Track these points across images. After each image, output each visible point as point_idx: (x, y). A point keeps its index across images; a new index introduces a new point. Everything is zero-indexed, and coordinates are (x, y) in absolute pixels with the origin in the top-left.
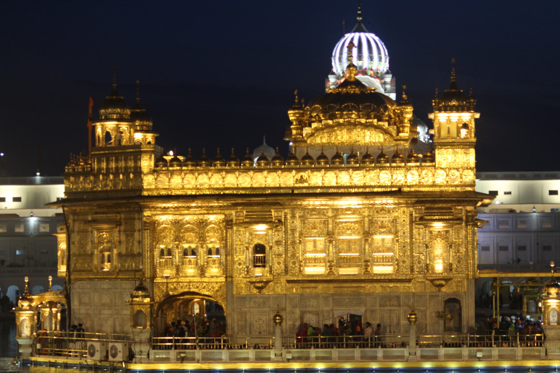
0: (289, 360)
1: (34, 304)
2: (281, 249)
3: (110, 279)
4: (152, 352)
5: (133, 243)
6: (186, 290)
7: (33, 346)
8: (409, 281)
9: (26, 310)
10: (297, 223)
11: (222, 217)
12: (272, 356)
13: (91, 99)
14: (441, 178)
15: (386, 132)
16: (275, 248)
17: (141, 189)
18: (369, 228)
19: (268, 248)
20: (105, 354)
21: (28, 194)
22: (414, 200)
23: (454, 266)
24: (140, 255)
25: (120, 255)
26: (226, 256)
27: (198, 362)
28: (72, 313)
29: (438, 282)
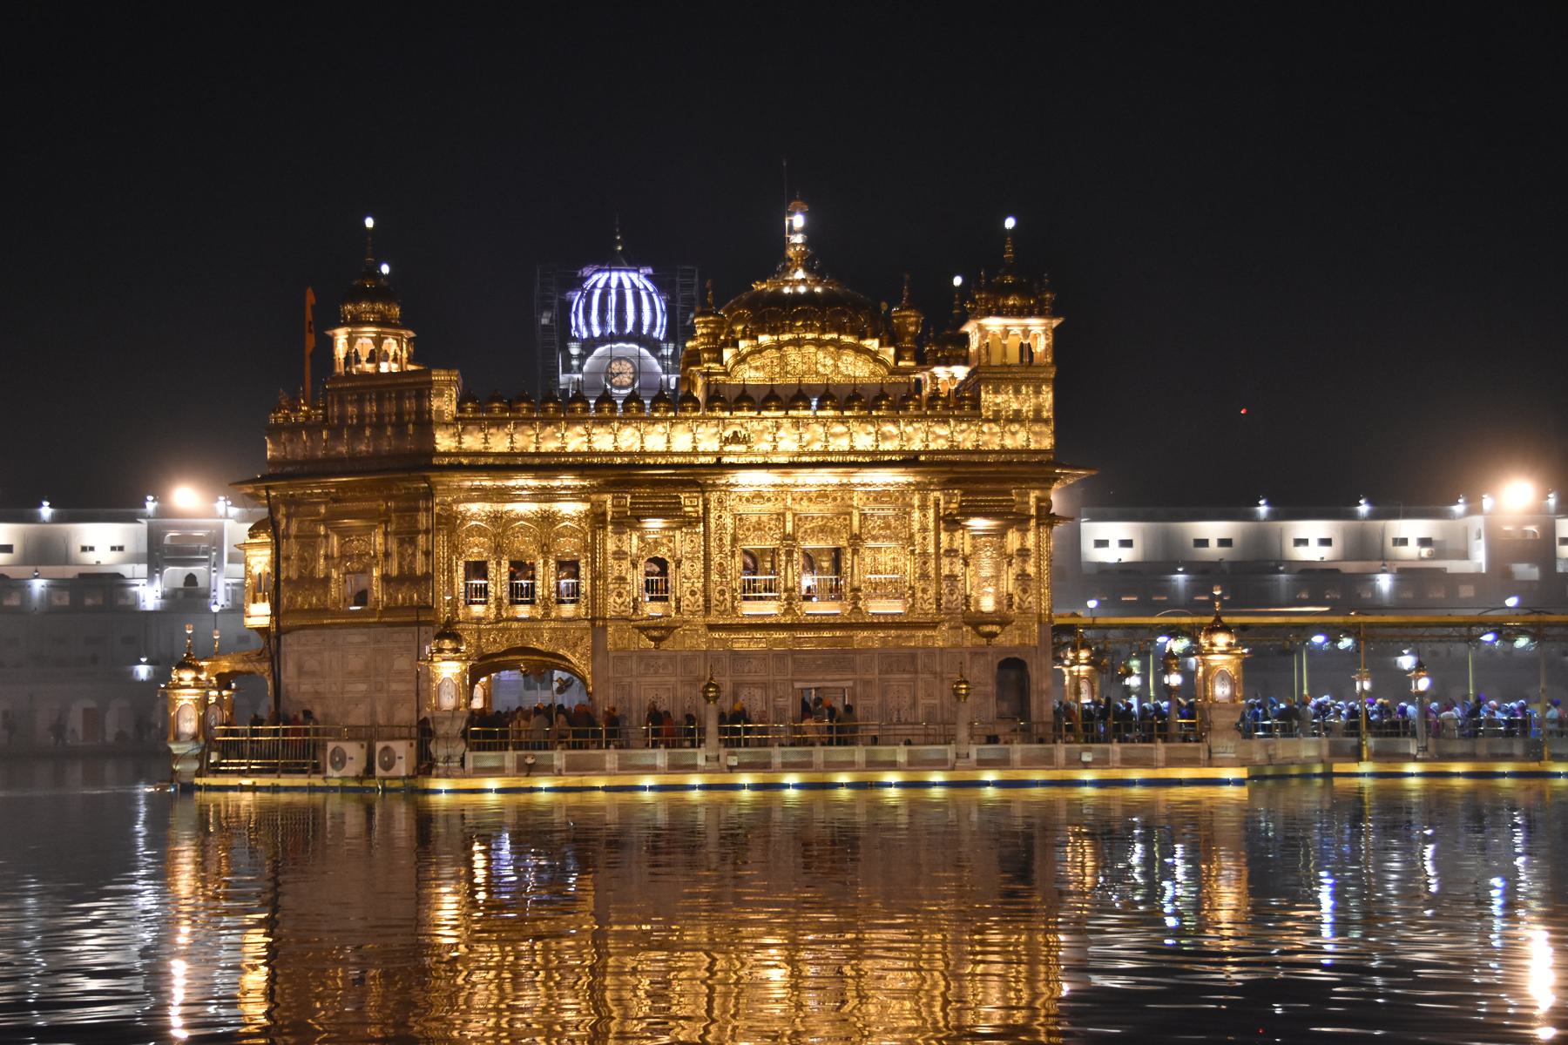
0: (731, 769)
1: (203, 676)
2: (699, 566)
3: (367, 625)
4: (470, 756)
5: (414, 555)
6: (519, 643)
7: (202, 757)
8: (934, 625)
9: (188, 687)
10: (728, 520)
11: (583, 507)
12: (701, 761)
14: (993, 438)
15: (874, 356)
19: (672, 566)
21: (26, 539)
23: (1016, 599)
24: (428, 577)
25: (386, 578)
26: (593, 580)
27: (560, 774)
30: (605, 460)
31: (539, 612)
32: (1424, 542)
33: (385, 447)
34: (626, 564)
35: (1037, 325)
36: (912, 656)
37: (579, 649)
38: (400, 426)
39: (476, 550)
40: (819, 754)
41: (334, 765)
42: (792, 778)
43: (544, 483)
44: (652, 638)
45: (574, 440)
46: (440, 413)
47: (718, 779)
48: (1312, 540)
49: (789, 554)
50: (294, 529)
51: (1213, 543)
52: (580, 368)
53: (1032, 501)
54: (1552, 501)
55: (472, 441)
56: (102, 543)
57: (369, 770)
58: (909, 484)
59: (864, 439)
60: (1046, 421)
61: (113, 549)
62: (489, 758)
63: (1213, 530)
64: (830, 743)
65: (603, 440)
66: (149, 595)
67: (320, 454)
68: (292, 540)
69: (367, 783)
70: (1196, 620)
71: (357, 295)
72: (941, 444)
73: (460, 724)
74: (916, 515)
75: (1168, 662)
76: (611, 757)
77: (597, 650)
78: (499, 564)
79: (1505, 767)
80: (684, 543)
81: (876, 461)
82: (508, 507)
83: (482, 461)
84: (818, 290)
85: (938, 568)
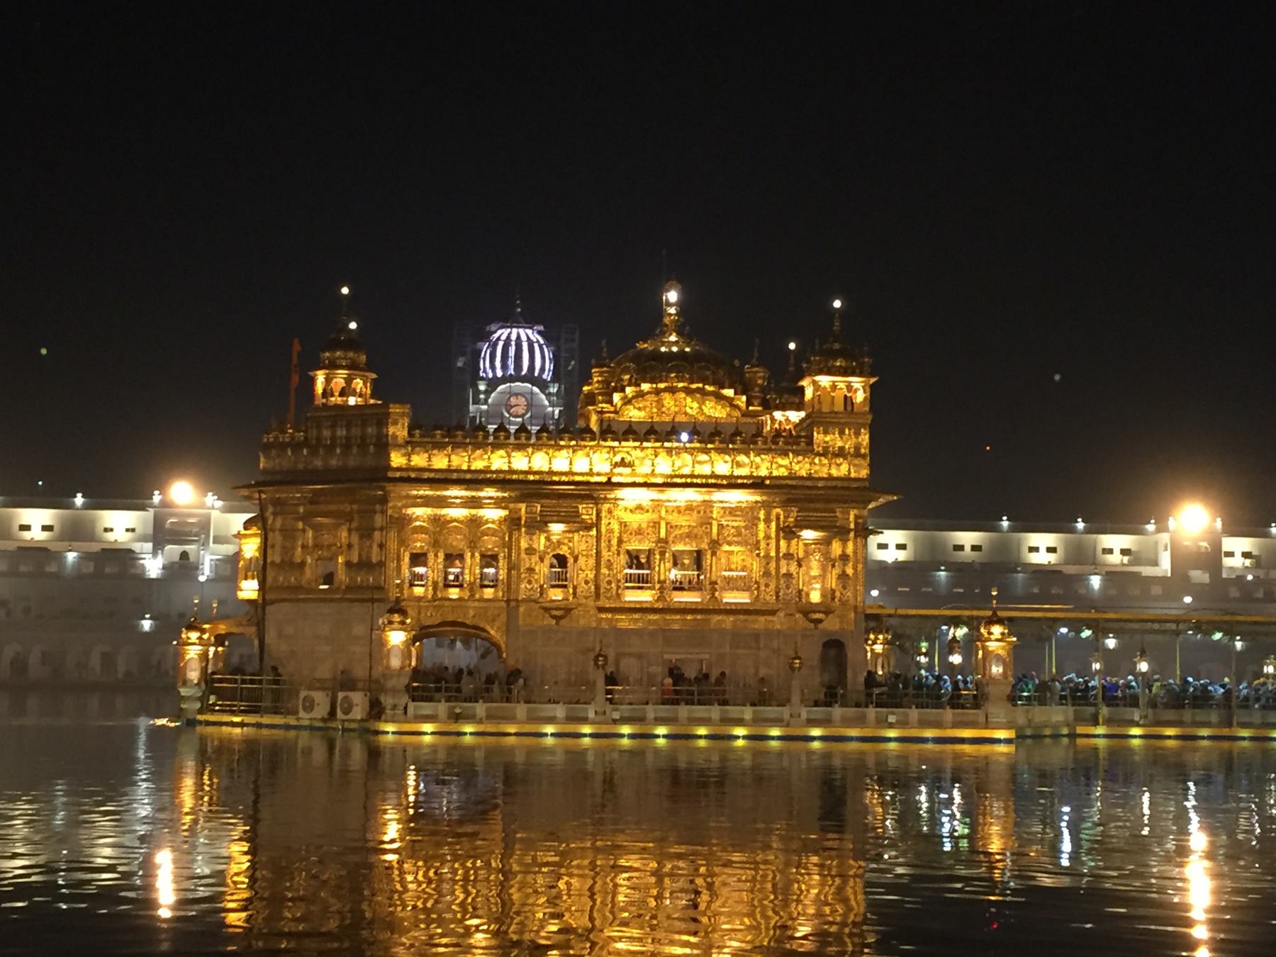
0: (615, 722)
1: (206, 636)
2: (592, 562)
4: (411, 706)
5: (371, 547)
7: (203, 699)
8: (773, 613)
10: (615, 527)
12: (591, 715)
13: (296, 341)
14: (822, 468)
16: (582, 561)
17: (389, 468)
18: (718, 534)
19: (571, 560)
20: (328, 709)
21: (63, 521)
22: (784, 497)
23: (838, 594)
24: (381, 564)
25: (348, 564)
26: (509, 570)
27: (480, 722)
28: (266, 649)
29: (818, 616)
30: (521, 477)
31: (466, 594)
32: (1124, 552)
33: (352, 462)
34: (535, 558)
35: (857, 382)
36: (756, 636)
37: (497, 624)
38: (363, 445)
39: (419, 545)
40: (683, 711)
41: (305, 709)
42: (662, 730)
43: (474, 494)
44: (554, 617)
45: (498, 461)
46: (395, 437)
47: (604, 729)
48: (1042, 548)
49: (662, 554)
50: (278, 524)
51: (968, 548)
52: (486, 402)
53: (852, 518)
54: (1219, 524)
55: (419, 460)
56: (119, 525)
57: (332, 713)
58: (757, 502)
59: (722, 466)
60: (864, 456)
61: (127, 530)
62: (426, 708)
63: (968, 538)
64: (693, 704)
65: (520, 461)
66: (153, 567)
67: (301, 466)
68: (277, 533)
69: (333, 725)
70: (975, 613)
71: (334, 345)
72: (783, 472)
73: (405, 681)
74: (762, 526)
75: (952, 646)
76: (521, 710)
77: (510, 628)
78: (436, 555)
79: (1205, 732)
80: (581, 543)
81: (732, 483)
82: (444, 511)
83: (426, 475)
84: (687, 350)
85: (778, 568)
